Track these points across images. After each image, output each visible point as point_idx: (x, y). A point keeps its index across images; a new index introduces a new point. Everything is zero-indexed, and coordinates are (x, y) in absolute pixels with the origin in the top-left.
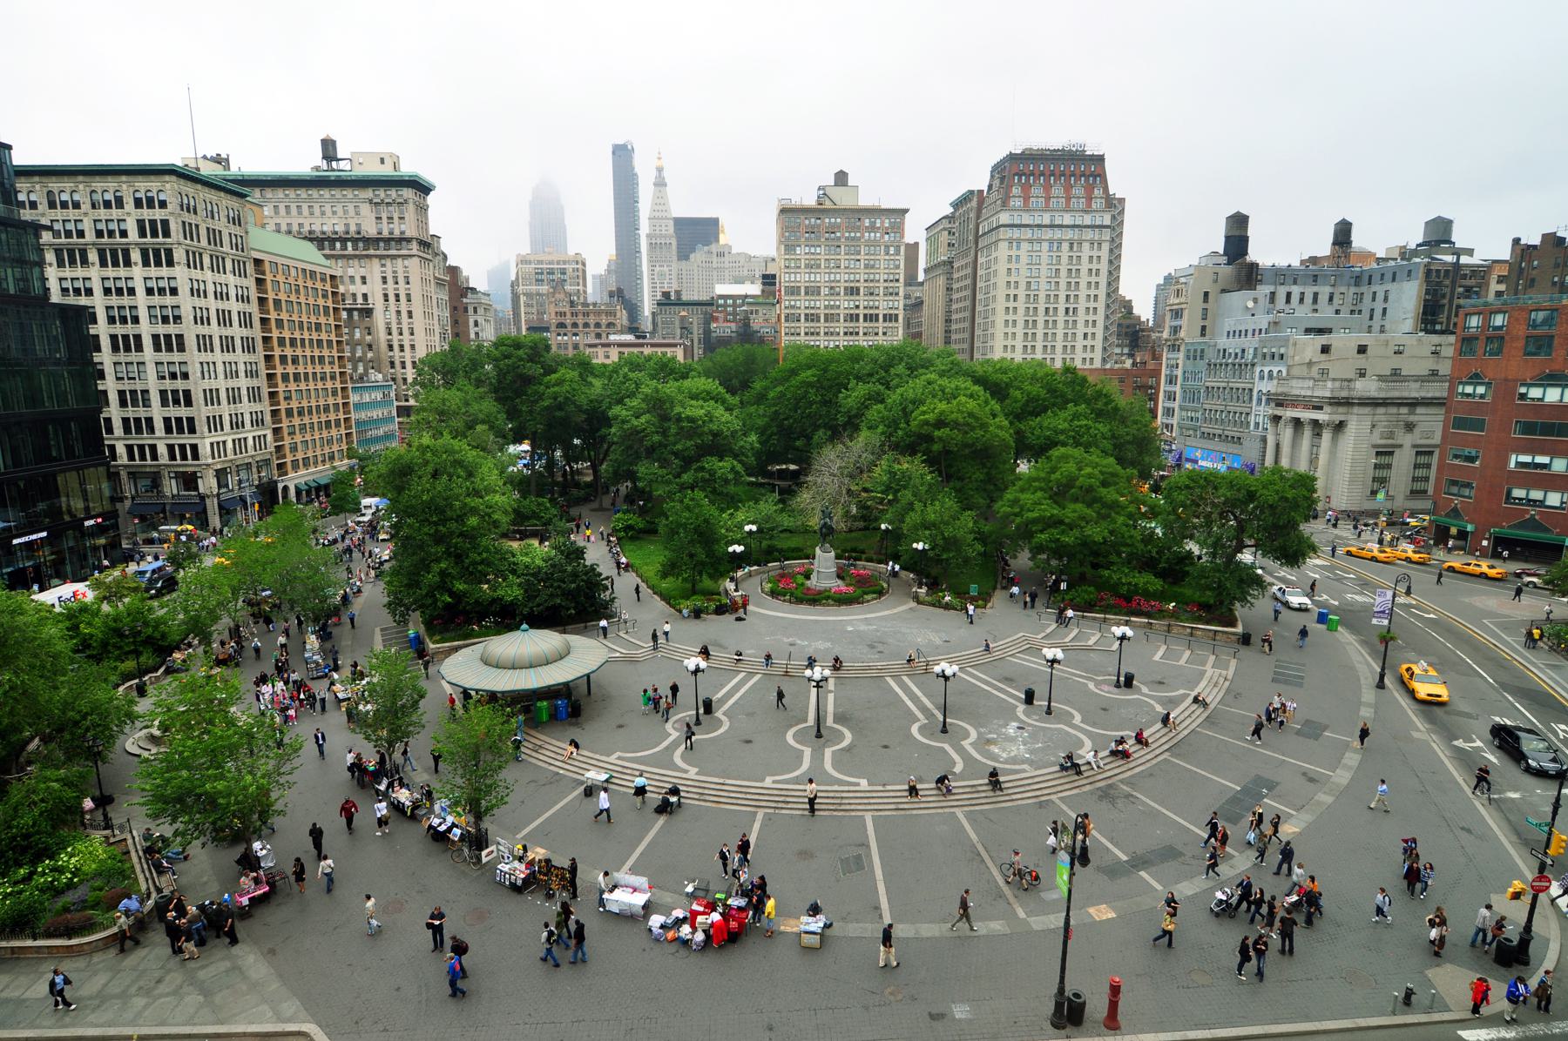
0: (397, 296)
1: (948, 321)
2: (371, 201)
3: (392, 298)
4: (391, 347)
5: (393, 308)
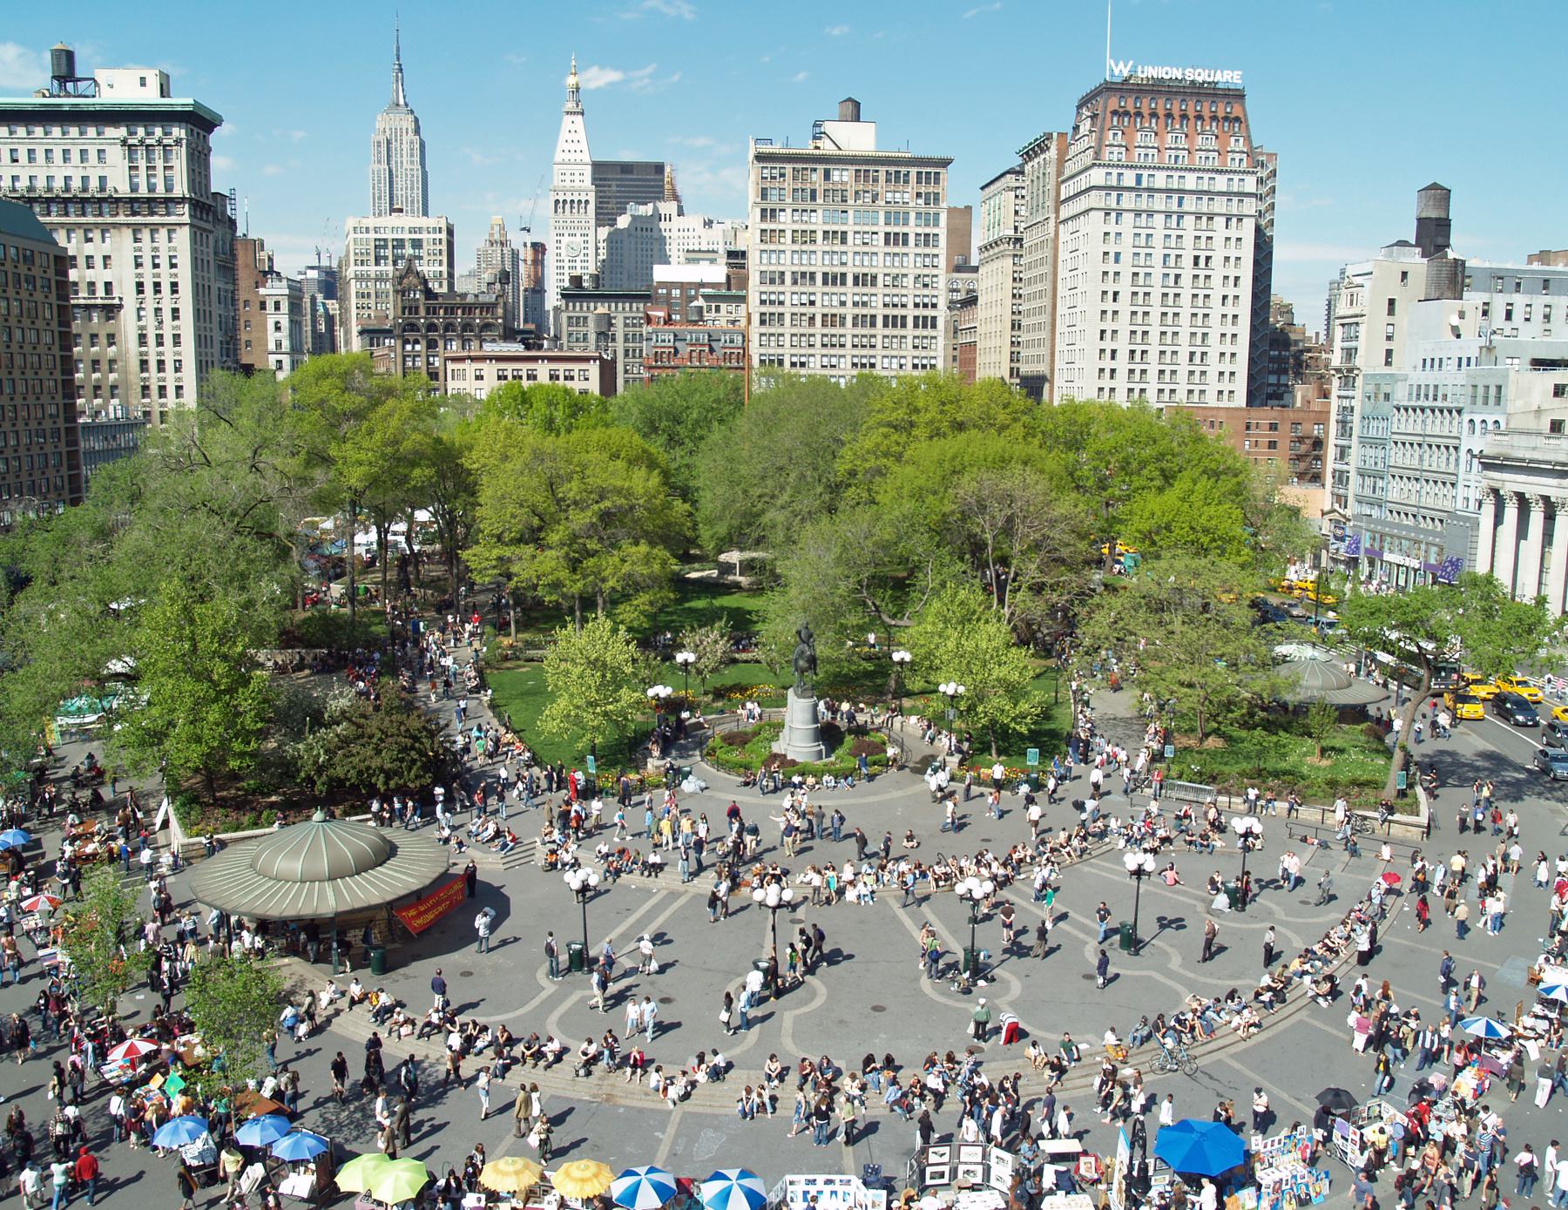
0: (157, 285)
1: (1015, 326)
2: (124, 142)
3: (149, 288)
4: (144, 365)
5: (150, 305)
